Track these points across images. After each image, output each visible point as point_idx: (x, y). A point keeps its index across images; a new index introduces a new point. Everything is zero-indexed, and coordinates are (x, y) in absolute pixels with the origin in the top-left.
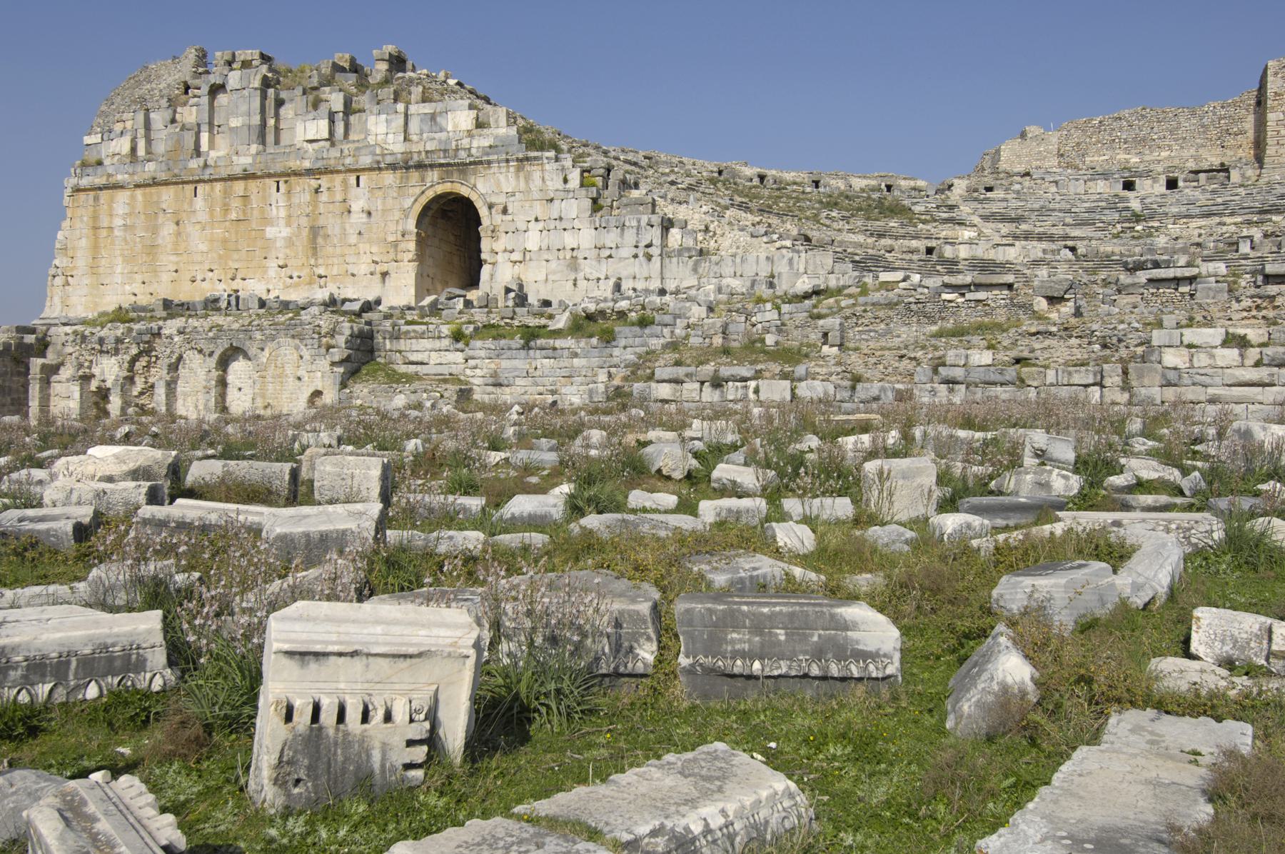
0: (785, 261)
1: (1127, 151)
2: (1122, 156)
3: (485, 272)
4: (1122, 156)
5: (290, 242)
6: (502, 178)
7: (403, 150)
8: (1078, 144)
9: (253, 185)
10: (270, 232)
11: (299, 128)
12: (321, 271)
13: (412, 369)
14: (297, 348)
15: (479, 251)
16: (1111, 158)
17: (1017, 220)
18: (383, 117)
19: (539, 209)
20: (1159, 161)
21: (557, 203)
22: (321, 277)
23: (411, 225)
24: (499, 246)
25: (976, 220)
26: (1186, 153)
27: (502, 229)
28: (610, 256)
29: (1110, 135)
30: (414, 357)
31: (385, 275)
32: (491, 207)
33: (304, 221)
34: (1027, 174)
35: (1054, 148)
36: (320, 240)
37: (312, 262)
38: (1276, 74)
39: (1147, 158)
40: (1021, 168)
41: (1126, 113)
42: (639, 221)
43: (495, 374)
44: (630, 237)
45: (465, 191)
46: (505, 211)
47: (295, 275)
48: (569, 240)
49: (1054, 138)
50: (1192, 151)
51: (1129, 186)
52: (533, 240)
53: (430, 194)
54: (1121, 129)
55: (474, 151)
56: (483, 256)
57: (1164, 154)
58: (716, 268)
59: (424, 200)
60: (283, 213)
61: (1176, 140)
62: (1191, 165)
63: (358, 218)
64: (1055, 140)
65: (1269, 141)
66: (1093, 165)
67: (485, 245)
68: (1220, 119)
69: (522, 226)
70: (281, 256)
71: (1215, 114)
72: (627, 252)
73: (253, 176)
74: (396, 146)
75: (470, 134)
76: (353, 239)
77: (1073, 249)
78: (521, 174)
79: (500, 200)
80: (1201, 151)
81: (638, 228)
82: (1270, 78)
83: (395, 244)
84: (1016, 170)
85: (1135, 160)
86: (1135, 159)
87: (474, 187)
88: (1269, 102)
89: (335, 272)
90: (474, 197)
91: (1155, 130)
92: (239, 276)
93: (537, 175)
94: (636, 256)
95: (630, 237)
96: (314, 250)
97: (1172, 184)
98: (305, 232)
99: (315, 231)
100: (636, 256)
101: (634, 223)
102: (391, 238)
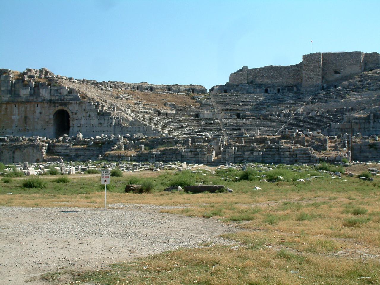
0: (142, 128)
1: (268, 79)
3: (71, 129)
5: (19, 120)
6: (75, 106)
7: (49, 98)
9: (9, 106)
10: (13, 117)
11: (22, 91)
12: (28, 128)
13: (57, 153)
14: (33, 149)
15: (69, 124)
17: (226, 104)
18: (44, 90)
19: (84, 114)
20: (276, 83)
21: (89, 113)
22: (27, 129)
23: (52, 117)
24: (75, 123)
25: (214, 104)
27: (75, 119)
28: (102, 126)
30: (58, 151)
31: (45, 129)
32: (72, 113)
33: (23, 115)
36: (28, 120)
37: (25, 125)
42: (108, 118)
43: (77, 154)
44: (106, 121)
45: (66, 109)
46: (76, 114)
47: (20, 129)
48: (92, 122)
51: (266, 91)
52: (83, 122)
53: (57, 110)
55: (68, 99)
56: (70, 125)
57: (278, 80)
58: (127, 129)
59: (55, 111)
60: (17, 113)
61: (281, 76)
62: (285, 84)
63: (37, 115)
67: (71, 122)
69: (80, 118)
70: (16, 123)
72: (105, 125)
73: (9, 103)
74: (48, 97)
75: (67, 95)
76: (36, 120)
77: (238, 116)
78: (80, 106)
79: (75, 111)
81: (108, 119)
83: (48, 122)
85: (270, 82)
87: (68, 108)
89: (31, 128)
90: (68, 111)
91: (275, 73)
92: (5, 128)
93: (84, 106)
94: (108, 126)
95: (106, 121)
96: (26, 123)
97: (279, 90)
98: (23, 117)
99: (26, 118)
100: (108, 126)
101: (107, 118)
102: (47, 120)
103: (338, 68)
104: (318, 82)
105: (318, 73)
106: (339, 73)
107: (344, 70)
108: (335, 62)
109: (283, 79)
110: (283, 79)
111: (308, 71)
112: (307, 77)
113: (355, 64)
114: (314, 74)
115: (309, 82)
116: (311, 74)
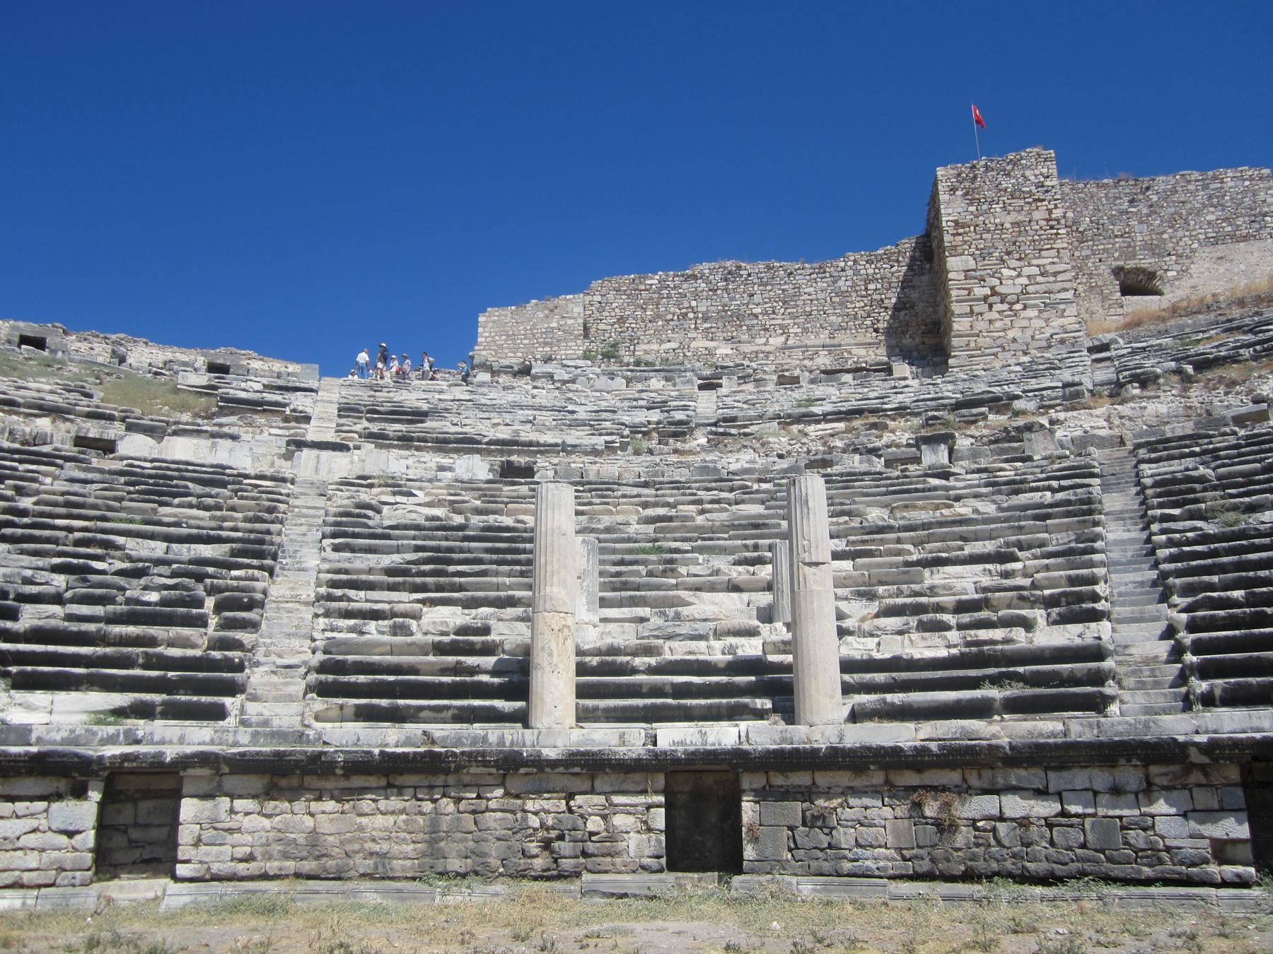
2: (700, 344)
4: (700, 344)
8: (621, 320)
16: (682, 346)
26: (811, 340)
29: (679, 306)
34: (525, 371)
35: (576, 325)
38: (953, 190)
39: (747, 348)
40: (514, 360)
41: (705, 267)
49: (574, 307)
50: (824, 337)
54: (696, 296)
57: (777, 341)
64: (578, 309)
65: (956, 308)
66: (649, 358)
68: (868, 281)
71: (857, 273)
80: (841, 337)
82: (943, 197)
84: (505, 362)
86: (724, 350)
88: (947, 238)
91: (757, 298)
103: (1146, 262)
104: (1057, 323)
105: (1050, 269)
106: (1159, 293)
107: (1184, 272)
108: (1117, 229)
109: (805, 330)
110: (805, 330)
111: (983, 255)
112: (980, 291)
113: (1245, 238)
114: (1026, 271)
115: (998, 325)
116: (1006, 272)
